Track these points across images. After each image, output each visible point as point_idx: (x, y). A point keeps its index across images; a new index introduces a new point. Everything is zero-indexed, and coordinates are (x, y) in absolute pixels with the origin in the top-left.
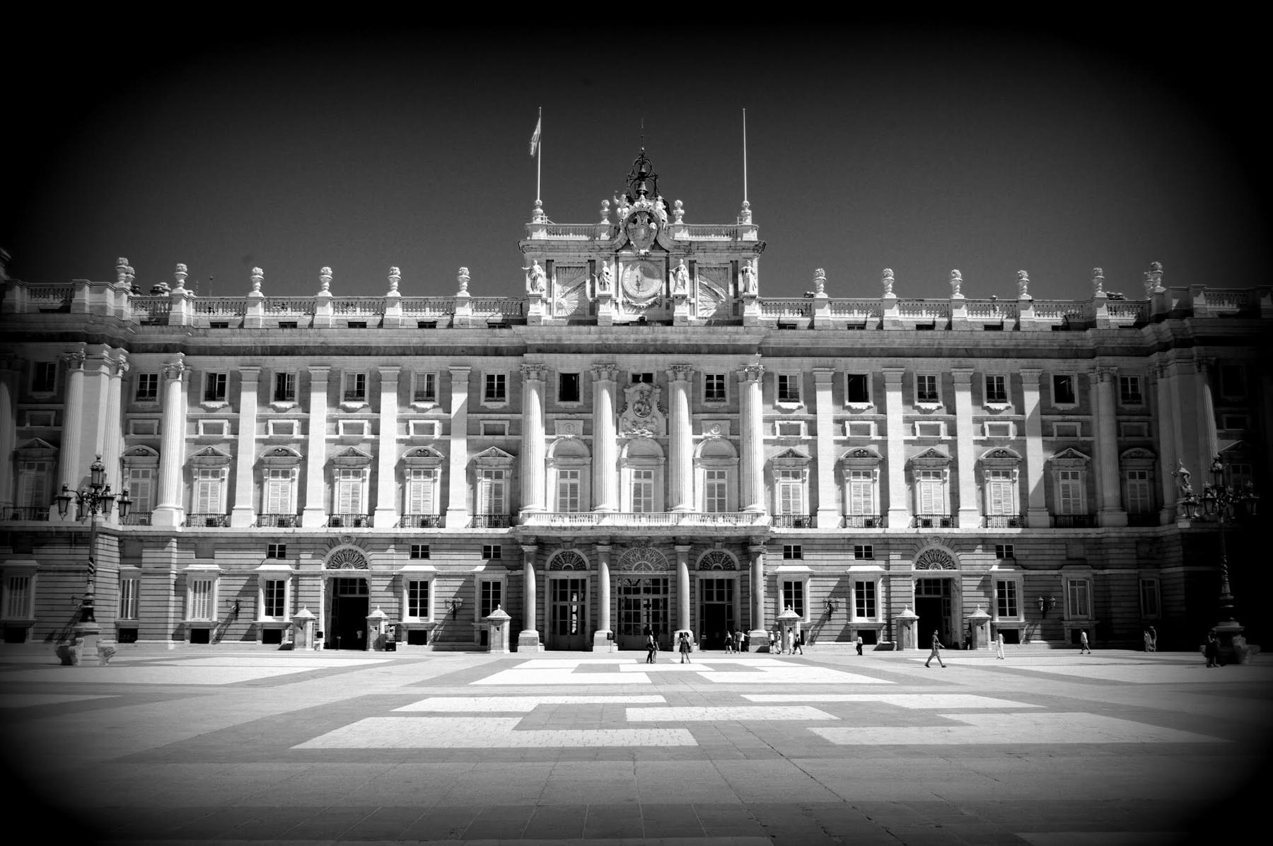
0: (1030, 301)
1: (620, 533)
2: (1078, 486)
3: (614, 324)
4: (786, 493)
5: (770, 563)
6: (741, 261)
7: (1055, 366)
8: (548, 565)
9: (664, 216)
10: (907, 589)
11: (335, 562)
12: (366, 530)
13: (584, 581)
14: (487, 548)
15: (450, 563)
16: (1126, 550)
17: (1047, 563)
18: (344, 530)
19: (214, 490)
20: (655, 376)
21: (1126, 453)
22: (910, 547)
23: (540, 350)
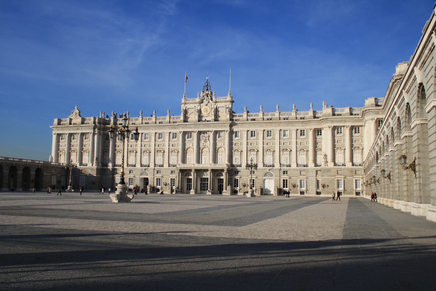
1: (196, 168)
2: (304, 157)
4: (236, 159)
6: (227, 105)
7: (300, 127)
8: (184, 175)
11: (142, 174)
13: (192, 179)
16: (313, 173)
17: (295, 175)
18: (143, 167)
19: (120, 158)
20: (208, 132)
21: (316, 149)
22: (262, 171)
23: (183, 128)
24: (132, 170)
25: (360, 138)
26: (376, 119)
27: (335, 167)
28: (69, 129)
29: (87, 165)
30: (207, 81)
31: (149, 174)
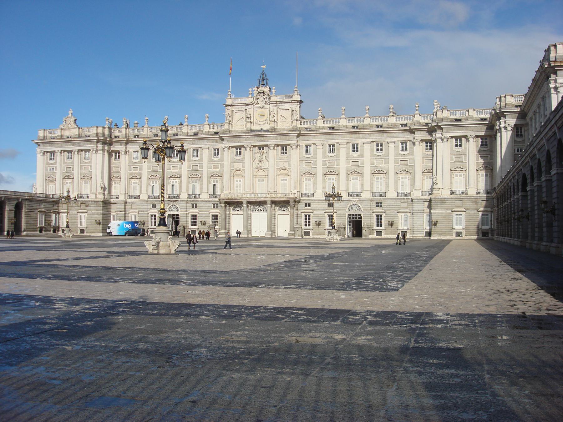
0: (393, 116)
1: (248, 200)
3: (252, 131)
4: (306, 186)
5: (300, 209)
6: (293, 106)
9: (269, 93)
10: (344, 217)
12: (178, 199)
14: (214, 204)
15: (203, 209)
16: (419, 204)
17: (393, 208)
18: (171, 199)
19: (136, 187)
20: (265, 147)
23: (228, 141)
24: (155, 203)
25: (488, 153)
26: (513, 126)
27: (452, 196)
28: (60, 144)
29: (88, 197)
30: (263, 71)
31: (179, 208)
